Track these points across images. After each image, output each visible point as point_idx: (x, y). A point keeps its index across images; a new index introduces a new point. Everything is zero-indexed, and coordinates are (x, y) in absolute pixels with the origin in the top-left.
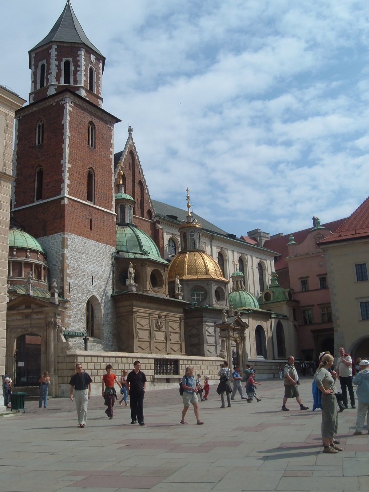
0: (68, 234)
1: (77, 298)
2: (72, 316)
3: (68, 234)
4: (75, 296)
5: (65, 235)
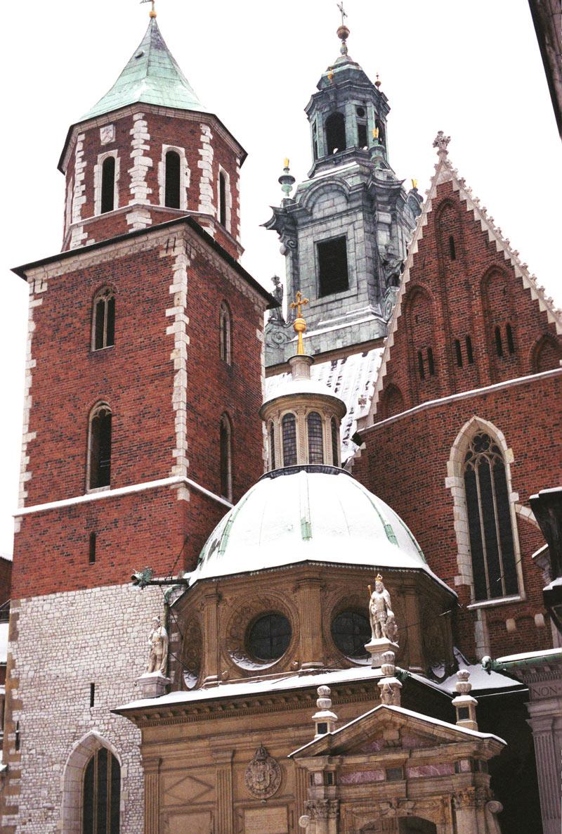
0: (18, 605)
1: (38, 757)
2: (24, 807)
3: (18, 605)
4: (33, 752)
5: (11, 610)
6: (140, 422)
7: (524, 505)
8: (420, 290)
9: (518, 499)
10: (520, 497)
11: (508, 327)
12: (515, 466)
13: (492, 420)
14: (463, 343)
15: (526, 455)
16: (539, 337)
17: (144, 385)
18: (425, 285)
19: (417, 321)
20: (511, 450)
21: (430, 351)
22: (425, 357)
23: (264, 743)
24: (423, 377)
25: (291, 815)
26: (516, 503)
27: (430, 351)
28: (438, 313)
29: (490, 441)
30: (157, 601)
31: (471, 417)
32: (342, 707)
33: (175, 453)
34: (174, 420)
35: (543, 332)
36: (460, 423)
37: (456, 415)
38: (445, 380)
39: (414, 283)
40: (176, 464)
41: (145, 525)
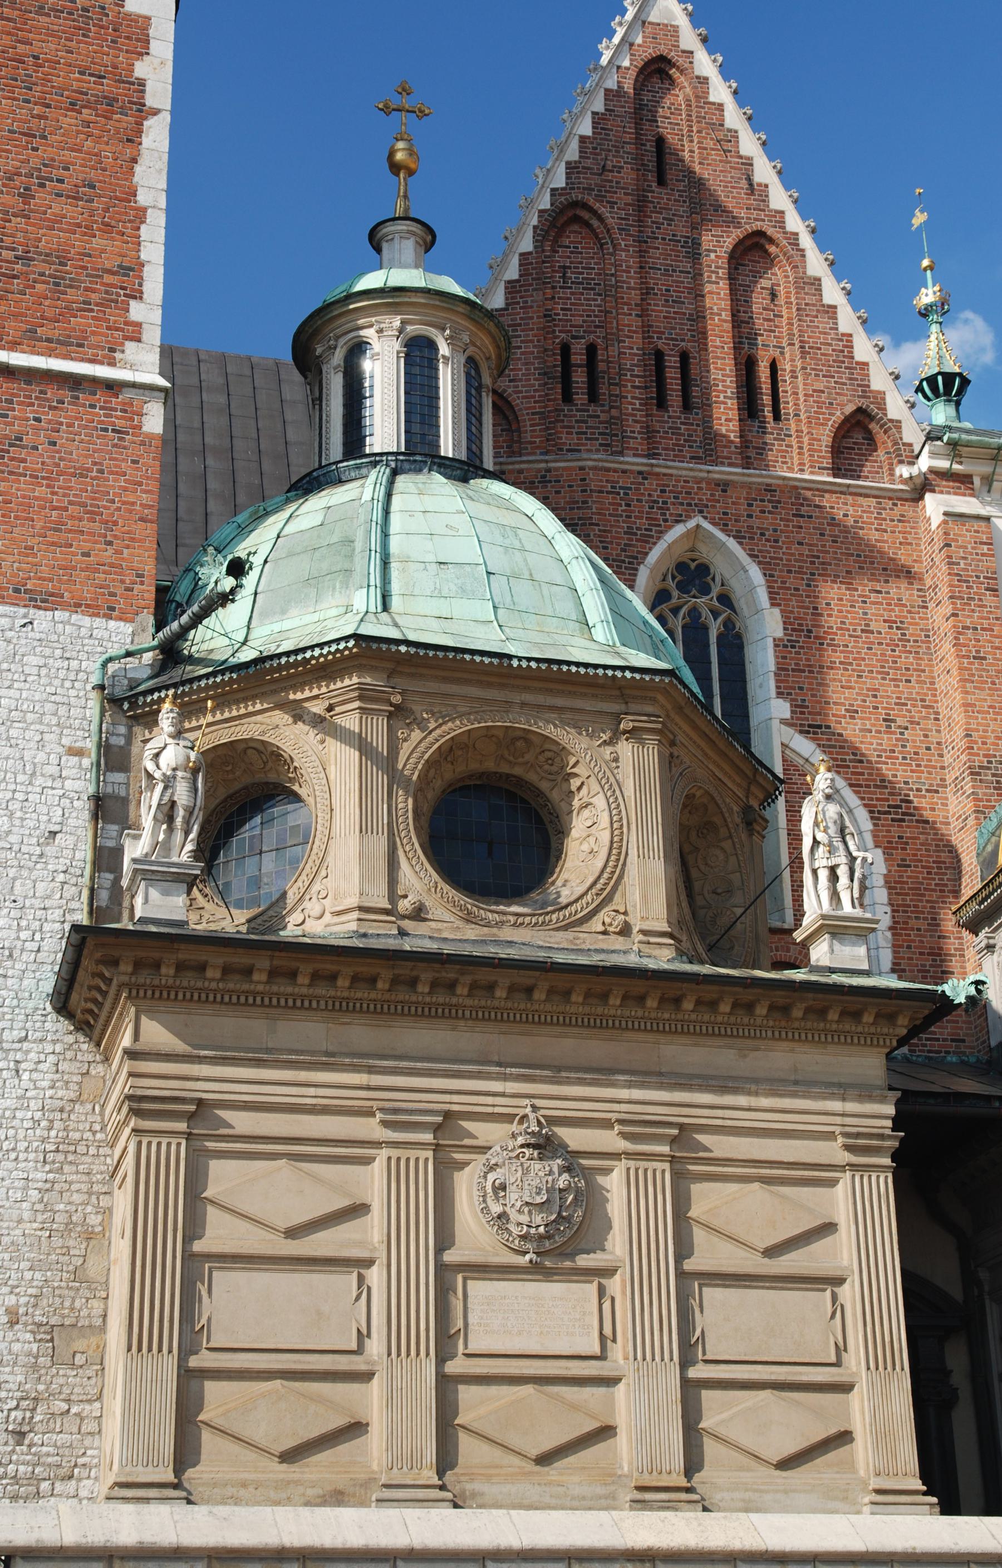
6: (27, 195)
7: (801, 732)
8: (586, 215)
9: (787, 715)
10: (792, 712)
11: (773, 367)
12: (785, 646)
13: (738, 537)
14: (672, 361)
15: (810, 631)
16: (850, 409)
17: (48, 106)
18: (604, 210)
19: (564, 277)
20: (776, 611)
21: (591, 350)
22: (578, 358)
23: (539, 1103)
24: (567, 397)
25: (607, 1306)
26: (783, 722)
27: (591, 350)
28: (631, 279)
29: (713, 579)
30: (62, 674)
31: (690, 517)
32: (757, 1049)
33: (137, 311)
34: (138, 229)
35: (863, 403)
36: (666, 521)
37: (655, 502)
38: (636, 422)
39: (576, 196)
40: (139, 340)
41: (33, 462)
